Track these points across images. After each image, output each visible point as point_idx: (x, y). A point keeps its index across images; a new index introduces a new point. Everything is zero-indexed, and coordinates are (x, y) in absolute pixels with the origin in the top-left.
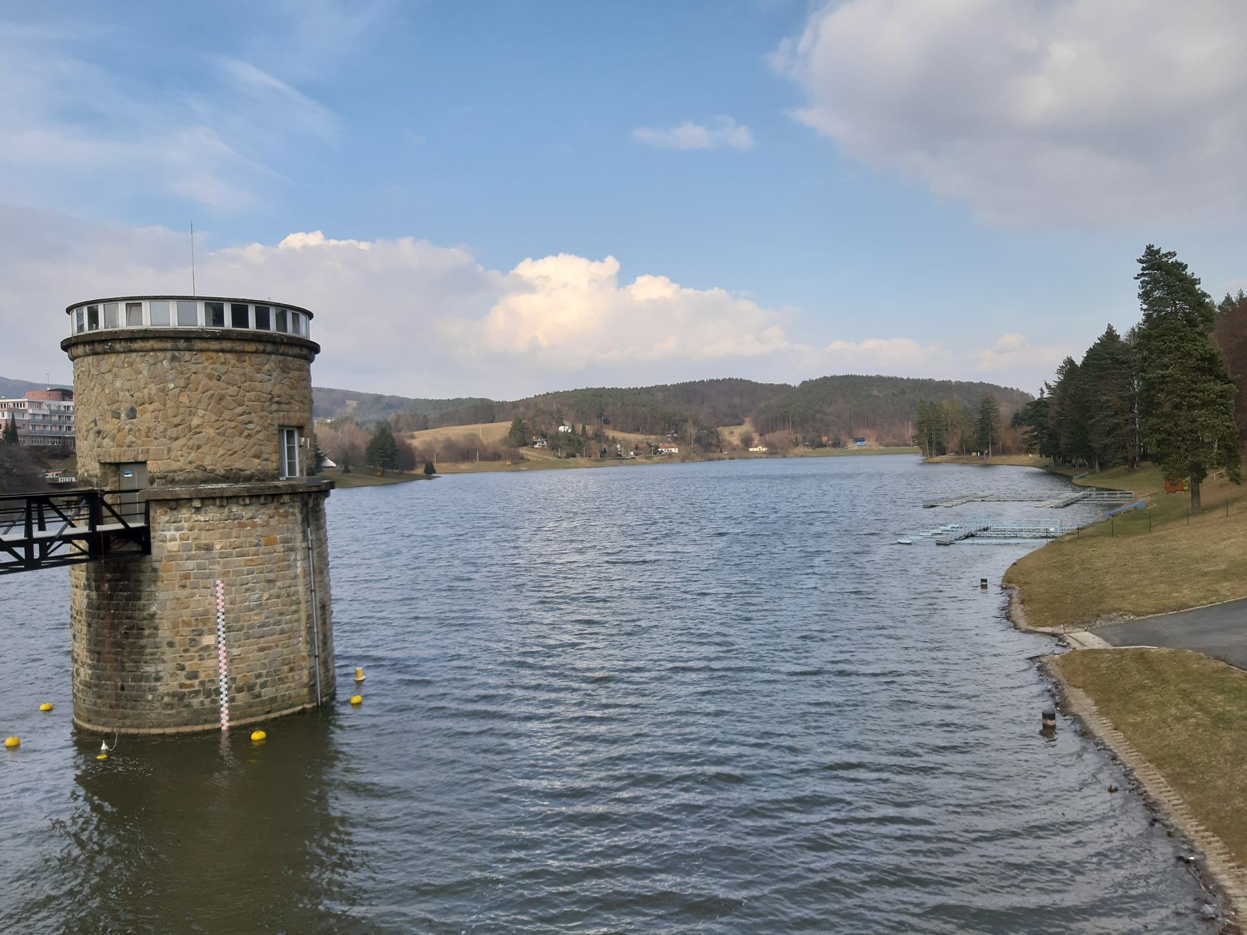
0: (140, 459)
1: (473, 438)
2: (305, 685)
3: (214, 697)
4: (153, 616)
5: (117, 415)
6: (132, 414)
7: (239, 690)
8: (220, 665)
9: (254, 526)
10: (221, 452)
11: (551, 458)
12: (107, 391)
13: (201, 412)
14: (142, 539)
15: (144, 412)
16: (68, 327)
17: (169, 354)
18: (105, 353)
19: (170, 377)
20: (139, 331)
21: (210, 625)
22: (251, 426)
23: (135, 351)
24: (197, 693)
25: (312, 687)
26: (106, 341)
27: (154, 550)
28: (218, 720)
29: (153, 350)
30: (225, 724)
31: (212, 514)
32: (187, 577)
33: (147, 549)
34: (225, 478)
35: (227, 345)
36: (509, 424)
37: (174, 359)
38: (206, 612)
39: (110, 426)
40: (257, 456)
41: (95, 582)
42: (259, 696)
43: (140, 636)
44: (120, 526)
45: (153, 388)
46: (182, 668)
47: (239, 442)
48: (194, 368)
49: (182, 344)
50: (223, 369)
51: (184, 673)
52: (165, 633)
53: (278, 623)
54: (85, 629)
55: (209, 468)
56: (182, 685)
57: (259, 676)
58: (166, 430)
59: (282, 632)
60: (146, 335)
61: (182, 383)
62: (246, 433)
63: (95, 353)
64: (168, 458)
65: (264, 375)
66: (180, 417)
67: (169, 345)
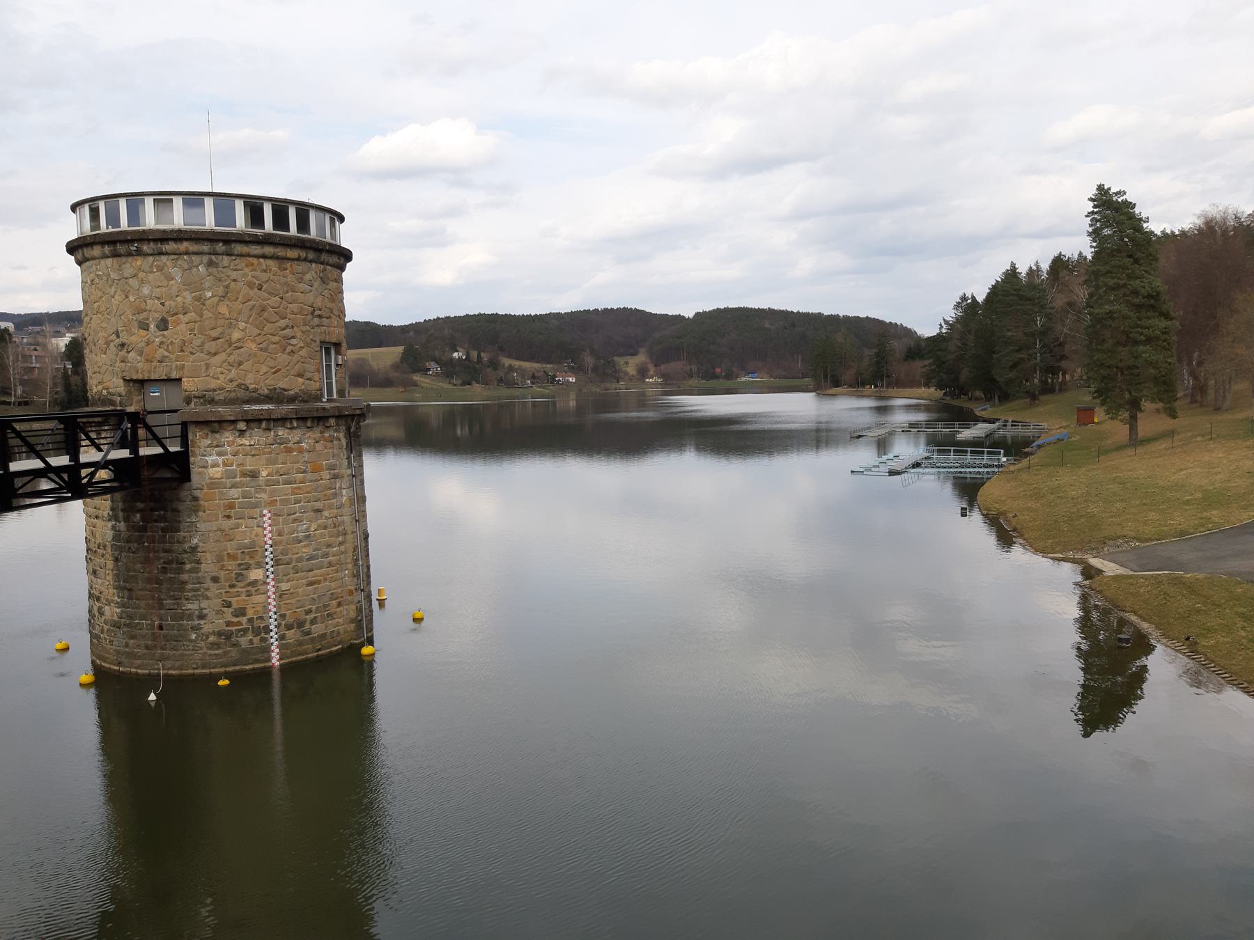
0: (174, 375)
1: (362, 362)
2: (352, 621)
3: (263, 635)
4: (194, 549)
5: (144, 326)
6: (163, 325)
7: (289, 627)
9: (301, 451)
10: (264, 369)
11: (446, 386)
12: (132, 298)
13: (242, 325)
14: (178, 466)
15: (178, 323)
16: (73, 227)
17: (205, 259)
18: (130, 254)
19: (207, 285)
20: (172, 231)
21: (258, 558)
22: (294, 341)
23: (167, 254)
24: (245, 631)
26: (132, 241)
27: (194, 477)
28: (269, 659)
29: (187, 253)
30: (275, 661)
31: (256, 437)
32: (231, 506)
33: (185, 475)
35: (269, 250)
36: (400, 349)
37: (211, 264)
38: (253, 545)
39: (137, 338)
40: (300, 375)
41: (125, 512)
42: (309, 633)
43: (180, 571)
44: (159, 450)
45: (188, 297)
46: (229, 605)
47: (283, 358)
48: (234, 275)
49: (220, 247)
50: (264, 276)
51: (231, 610)
52: (208, 567)
53: (325, 555)
54: (110, 564)
55: (251, 387)
56: (228, 624)
57: (309, 612)
58: (203, 344)
59: (330, 565)
60: (178, 236)
61: (221, 291)
62: (289, 349)
63: (115, 255)
64: (208, 375)
66: (220, 330)
67: (205, 247)
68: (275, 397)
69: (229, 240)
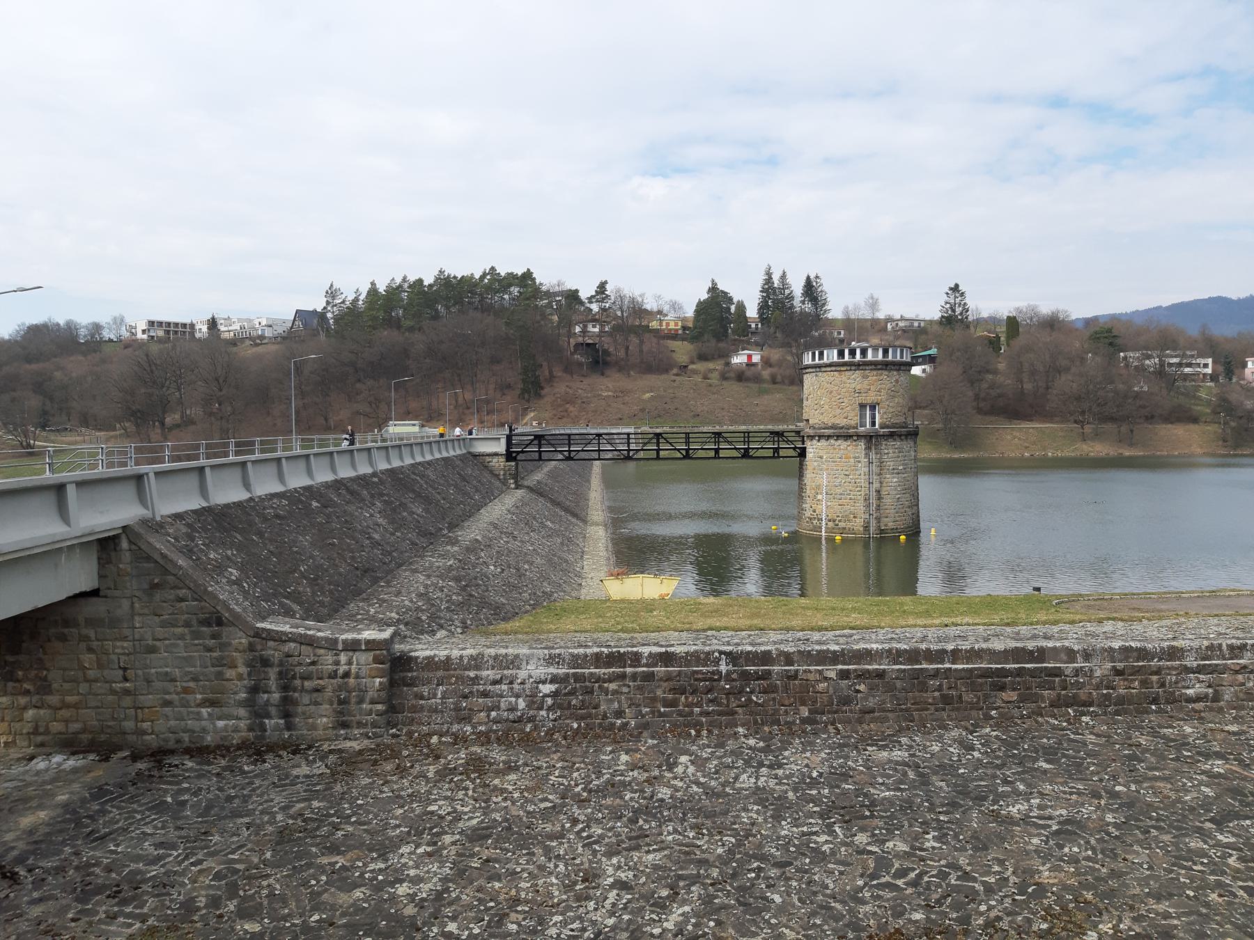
8: (823, 509)
25: (866, 528)
31: (823, 443)
34: (831, 428)
47: (839, 411)
65: (853, 380)
69: (819, 366)
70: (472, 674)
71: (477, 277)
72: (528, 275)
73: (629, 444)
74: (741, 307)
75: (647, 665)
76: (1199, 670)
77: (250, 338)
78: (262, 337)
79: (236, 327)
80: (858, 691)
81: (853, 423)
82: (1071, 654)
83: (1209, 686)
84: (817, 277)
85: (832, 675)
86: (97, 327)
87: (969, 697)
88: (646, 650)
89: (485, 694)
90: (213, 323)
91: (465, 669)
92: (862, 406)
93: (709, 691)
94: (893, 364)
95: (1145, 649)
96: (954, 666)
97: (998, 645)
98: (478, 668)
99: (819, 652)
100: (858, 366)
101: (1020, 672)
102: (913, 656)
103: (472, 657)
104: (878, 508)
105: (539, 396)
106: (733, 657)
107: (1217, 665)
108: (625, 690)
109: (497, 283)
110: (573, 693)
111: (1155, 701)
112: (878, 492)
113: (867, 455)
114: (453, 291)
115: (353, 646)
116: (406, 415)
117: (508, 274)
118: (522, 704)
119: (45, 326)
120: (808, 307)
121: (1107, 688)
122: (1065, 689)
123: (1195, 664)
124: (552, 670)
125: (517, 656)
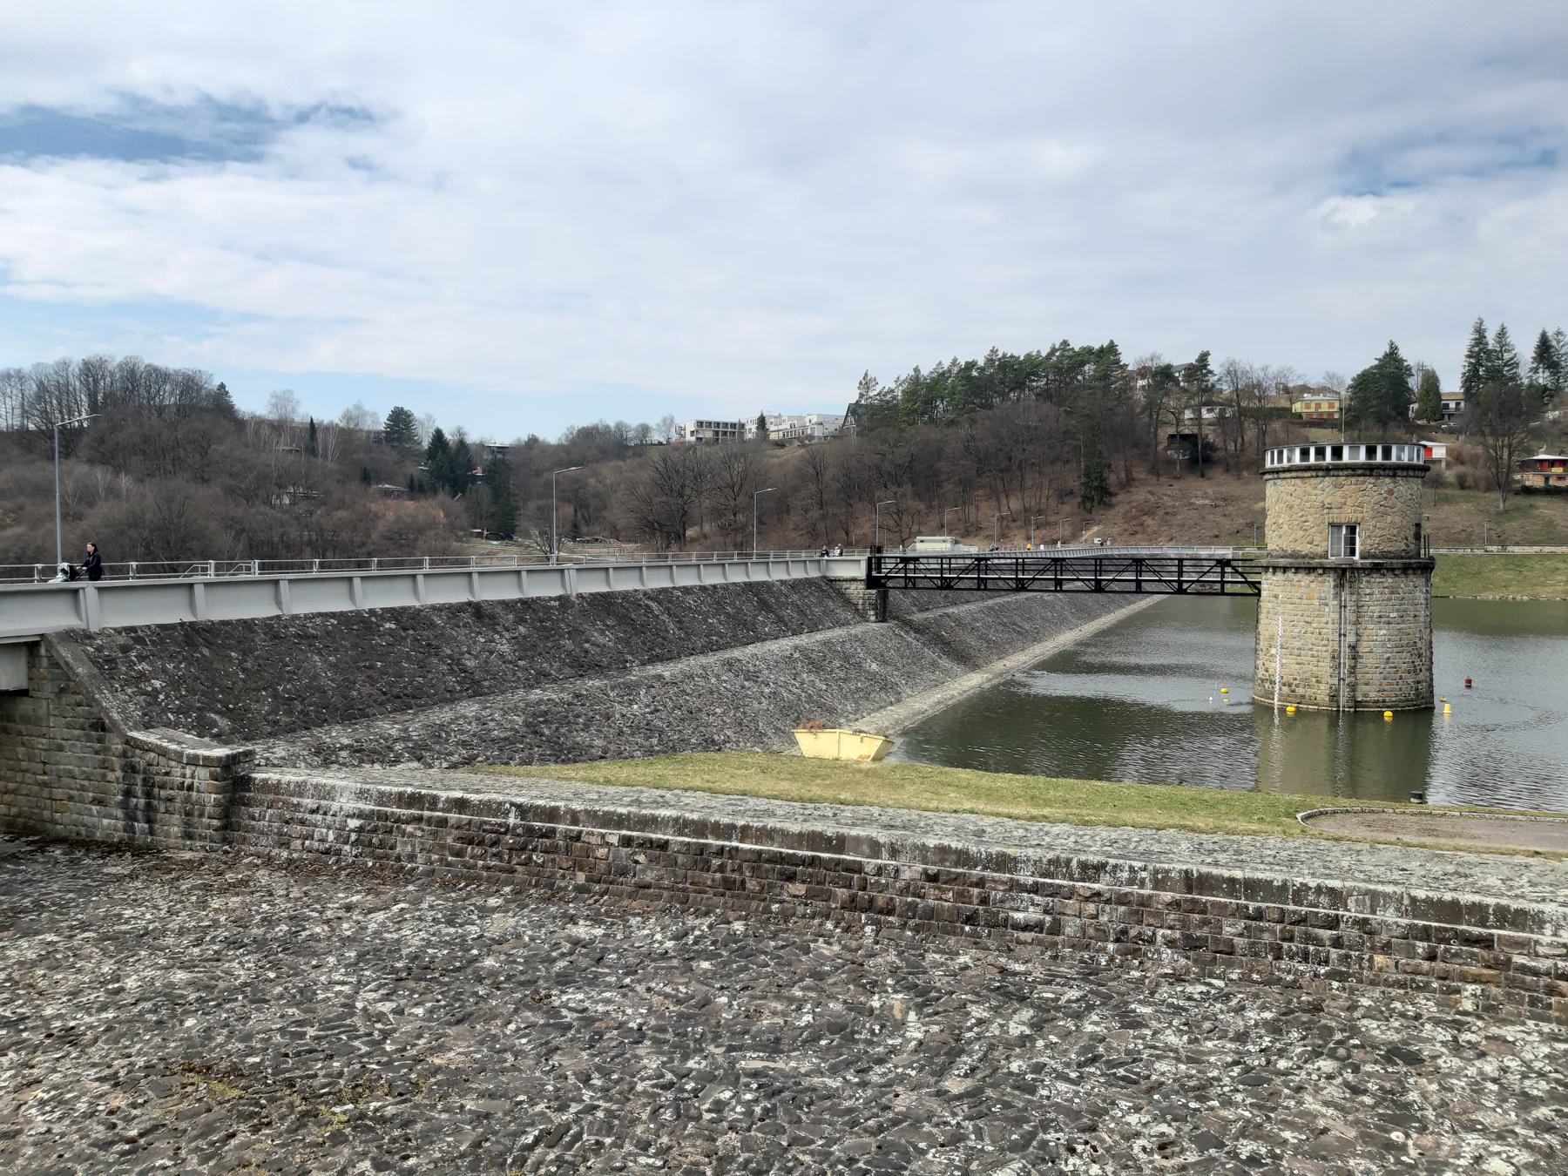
8: (1276, 668)
25: (1334, 697)
31: (1280, 576)
34: (1291, 556)
65: (1322, 490)
68: (1294, 555)
70: (295, 800)
71: (1044, 354)
72: (1112, 349)
73: (1180, 573)
74: (1431, 381)
75: (442, 810)
76: (1035, 889)
77: (798, 439)
78: (811, 437)
79: (786, 426)
80: (636, 862)
81: (1319, 550)
82: (875, 848)
83: (1046, 912)
84: (1559, 333)
85: (614, 840)
86: (645, 429)
87: (752, 885)
88: (443, 795)
89: (302, 822)
90: (762, 422)
91: (292, 795)
92: (1336, 526)
93: (494, 844)
94: (1346, 467)
95: (967, 853)
96: (741, 845)
97: (795, 828)
98: (301, 795)
99: (606, 813)
100: (1327, 471)
101: (813, 862)
102: (700, 828)
103: (298, 785)
104: (1353, 670)
105: (1110, 506)
106: (522, 810)
107: (1060, 886)
108: (419, 833)
109: (1067, 362)
110: (375, 830)
111: (971, 919)
112: (1353, 647)
113: (1337, 595)
114: (1009, 375)
115: (193, 761)
116: (939, 529)
117: (1083, 349)
118: (331, 837)
119: (595, 428)
120: (1543, 378)
121: (914, 895)
122: (864, 889)
123: (1031, 880)
124: (361, 805)
125: (333, 787)
